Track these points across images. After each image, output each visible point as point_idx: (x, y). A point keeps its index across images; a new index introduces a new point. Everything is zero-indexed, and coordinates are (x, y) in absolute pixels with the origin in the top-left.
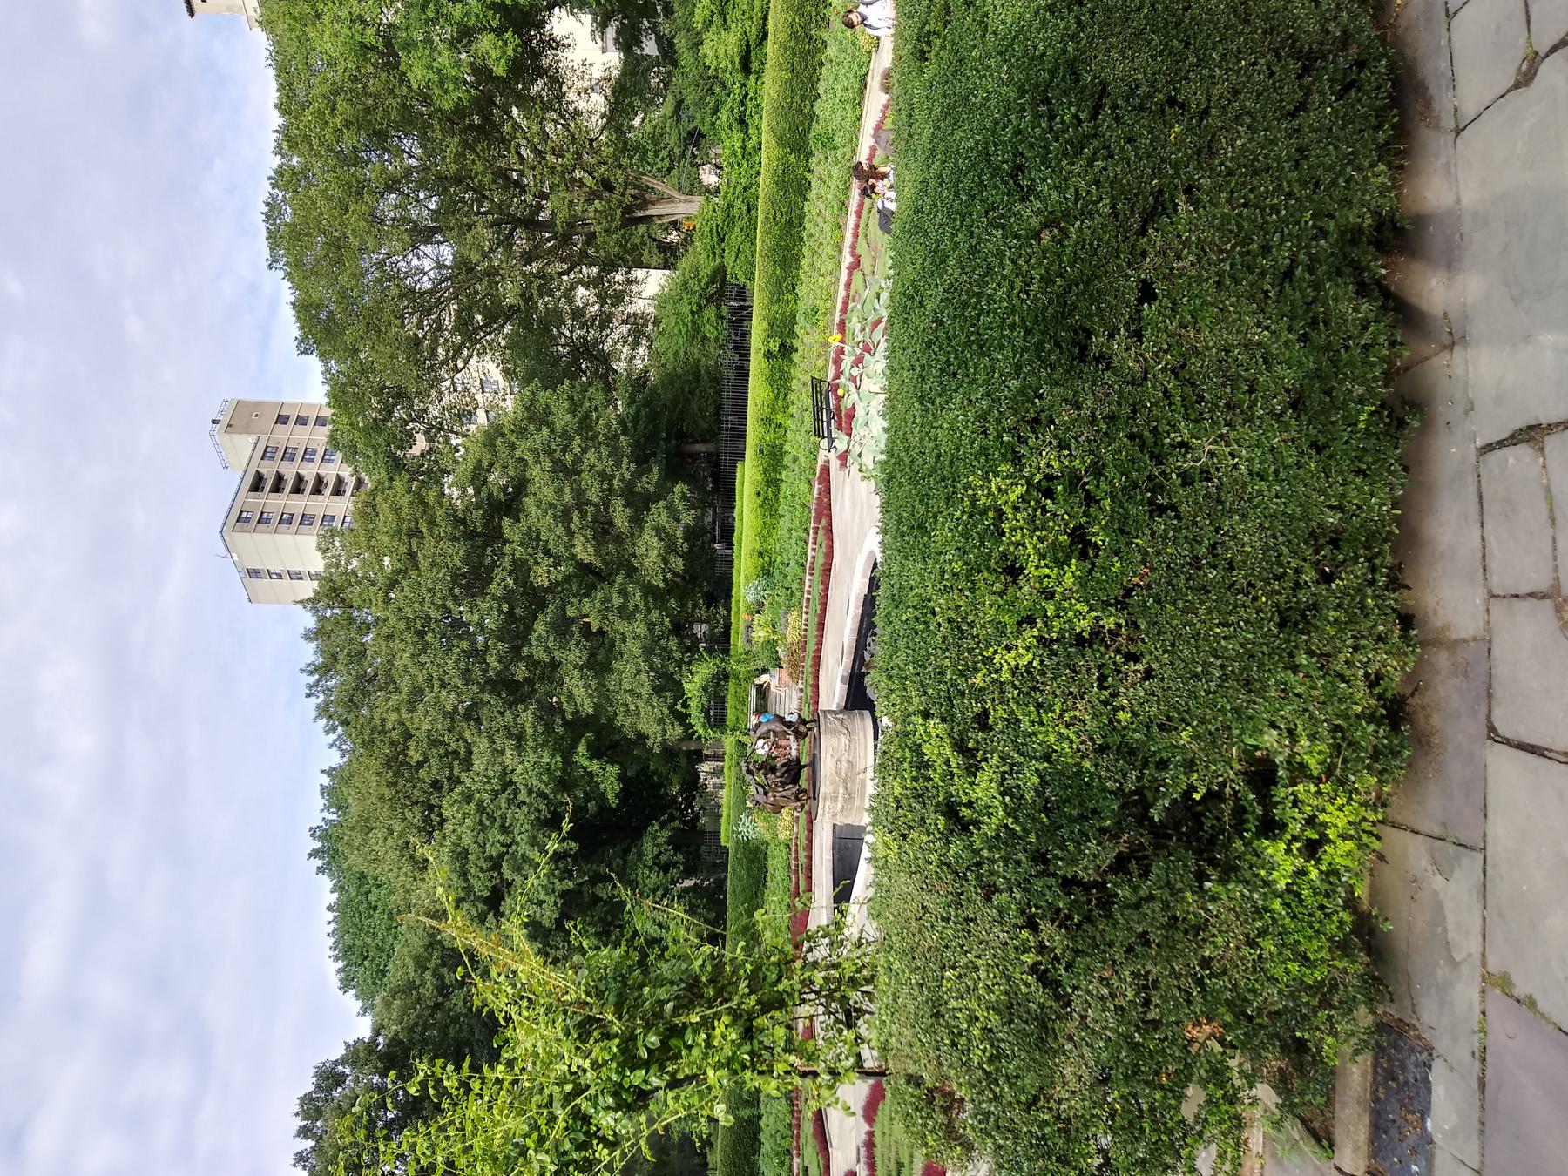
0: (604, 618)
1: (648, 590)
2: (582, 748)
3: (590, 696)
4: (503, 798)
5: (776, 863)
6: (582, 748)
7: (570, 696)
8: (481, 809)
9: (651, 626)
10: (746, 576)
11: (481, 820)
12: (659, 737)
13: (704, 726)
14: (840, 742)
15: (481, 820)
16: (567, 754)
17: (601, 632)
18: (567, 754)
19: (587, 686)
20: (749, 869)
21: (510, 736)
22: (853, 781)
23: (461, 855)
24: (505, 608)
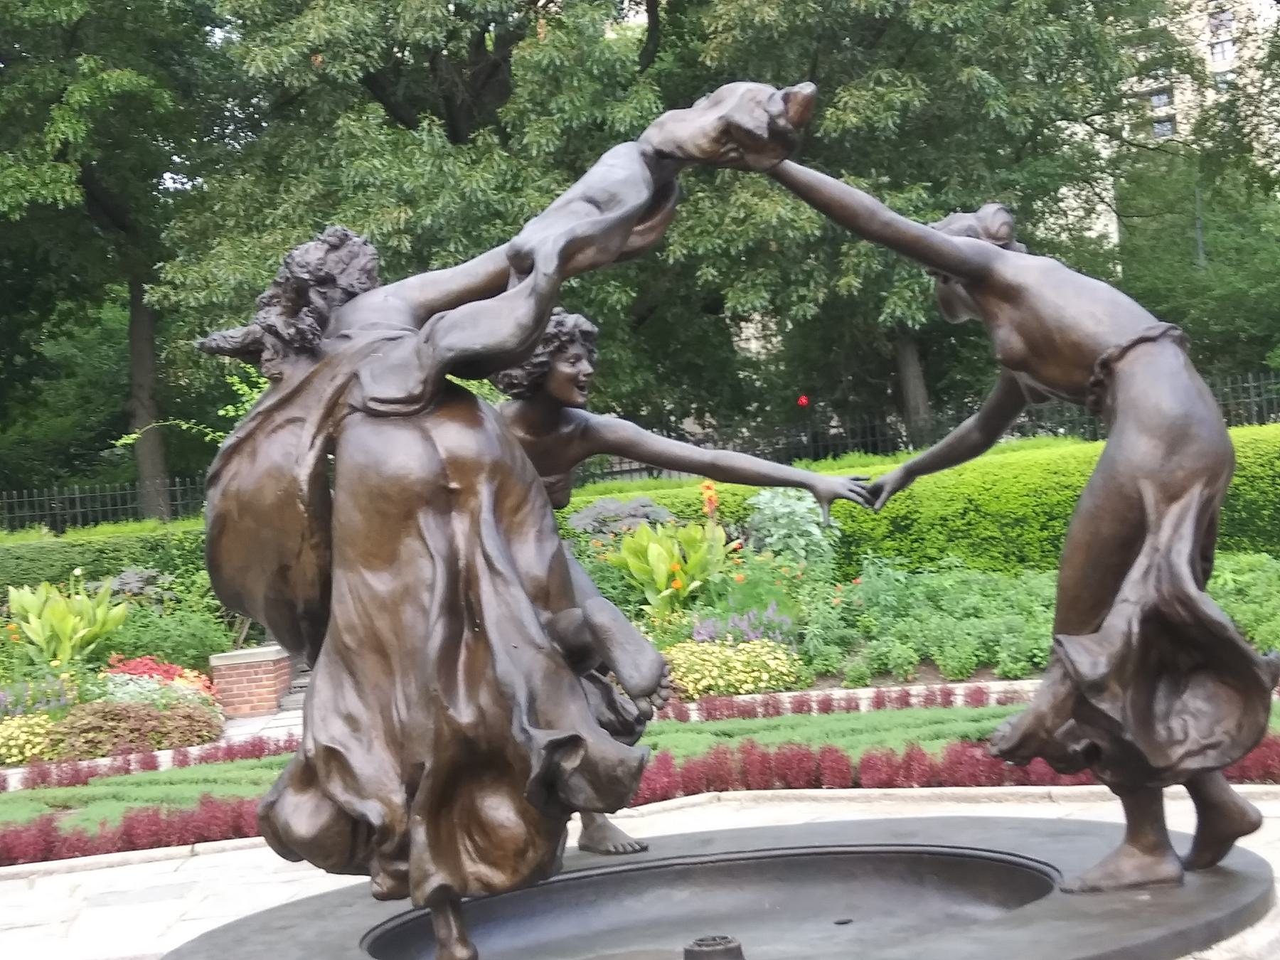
2: (120, 79)
6: (120, 79)
19: (331, 46)
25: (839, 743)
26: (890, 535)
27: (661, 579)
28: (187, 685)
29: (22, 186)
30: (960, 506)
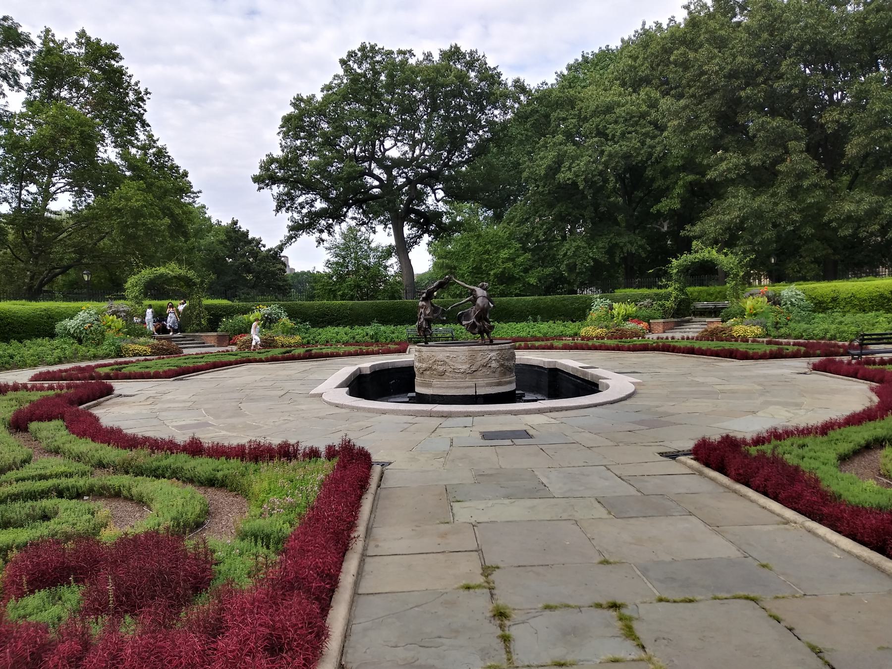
0: (787, 174)
1: (821, 209)
2: (691, 178)
3: (721, 175)
4: (650, 128)
5: (571, 327)
6: (691, 178)
7: (722, 160)
8: (643, 116)
9: (787, 214)
10: (815, 288)
11: (634, 117)
12: (691, 234)
13: (680, 265)
14: (462, 363)
15: (634, 117)
16: (683, 168)
17: (776, 174)
18: (683, 168)
19: (729, 170)
20: (579, 309)
21: (689, 121)
22: (431, 376)
23: (609, 109)
24: (795, 91)
25: (701, 346)
26: (831, 302)
27: (748, 309)
28: (644, 325)
29: (667, 206)
30: (850, 295)
